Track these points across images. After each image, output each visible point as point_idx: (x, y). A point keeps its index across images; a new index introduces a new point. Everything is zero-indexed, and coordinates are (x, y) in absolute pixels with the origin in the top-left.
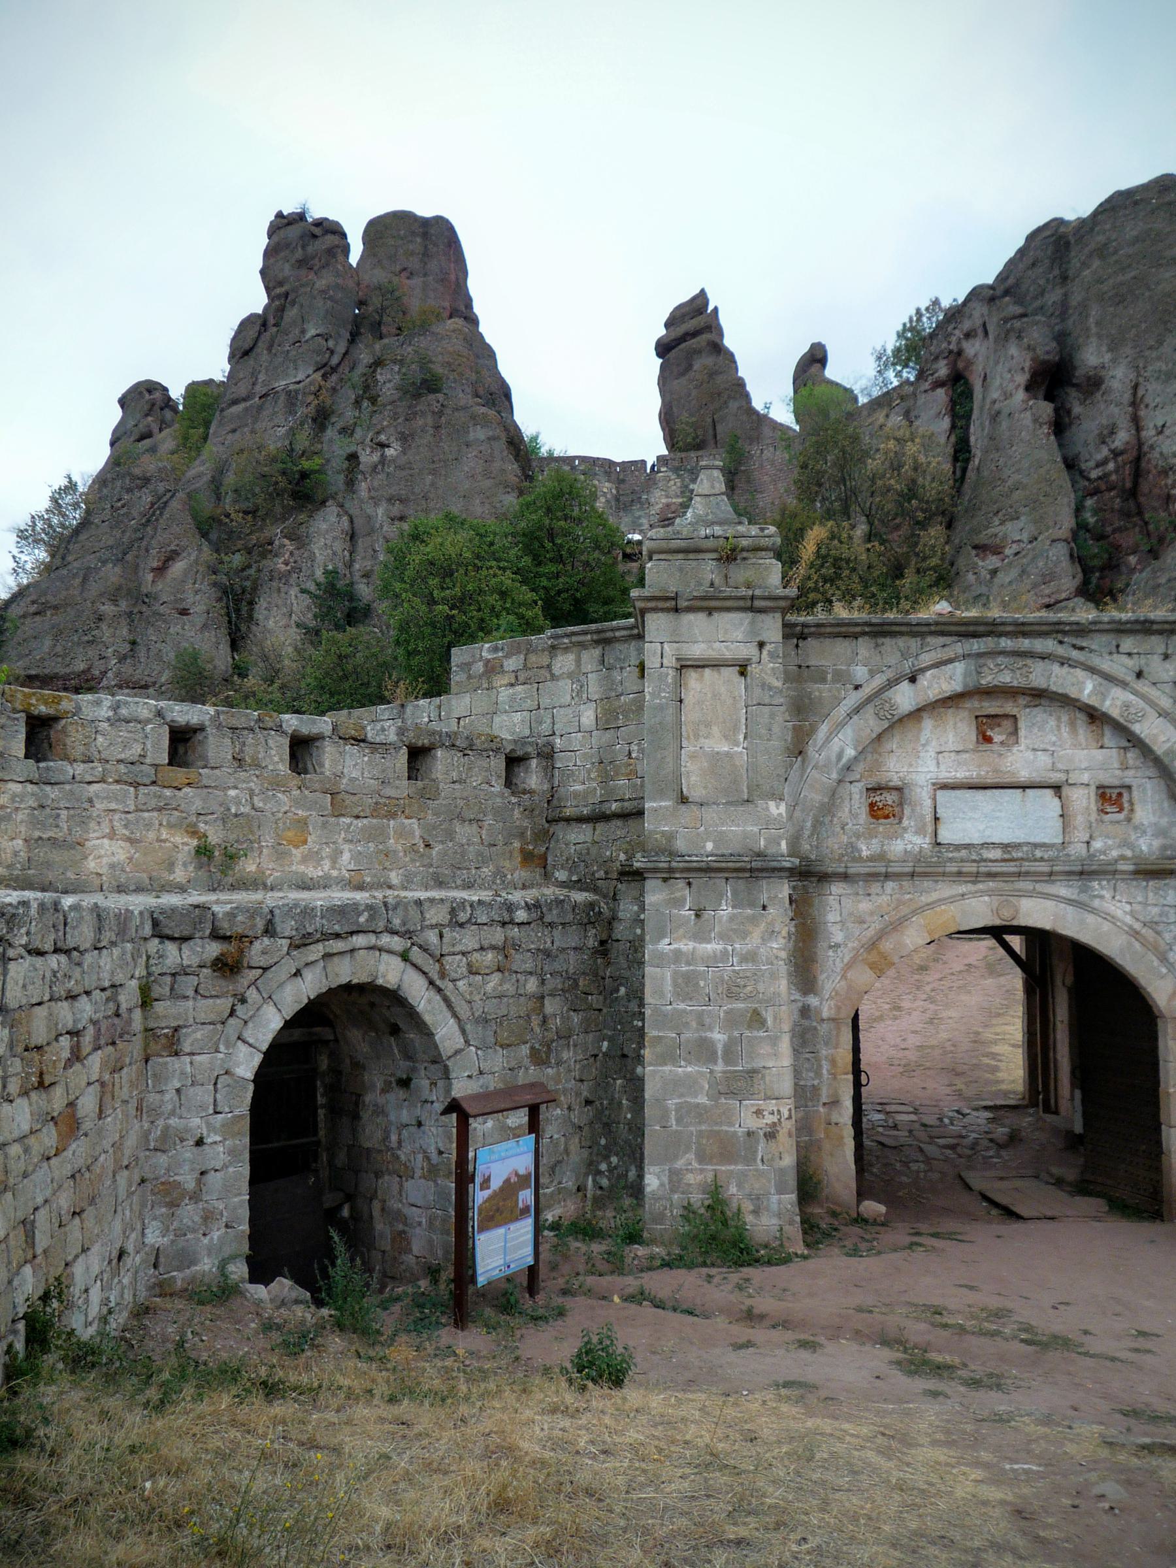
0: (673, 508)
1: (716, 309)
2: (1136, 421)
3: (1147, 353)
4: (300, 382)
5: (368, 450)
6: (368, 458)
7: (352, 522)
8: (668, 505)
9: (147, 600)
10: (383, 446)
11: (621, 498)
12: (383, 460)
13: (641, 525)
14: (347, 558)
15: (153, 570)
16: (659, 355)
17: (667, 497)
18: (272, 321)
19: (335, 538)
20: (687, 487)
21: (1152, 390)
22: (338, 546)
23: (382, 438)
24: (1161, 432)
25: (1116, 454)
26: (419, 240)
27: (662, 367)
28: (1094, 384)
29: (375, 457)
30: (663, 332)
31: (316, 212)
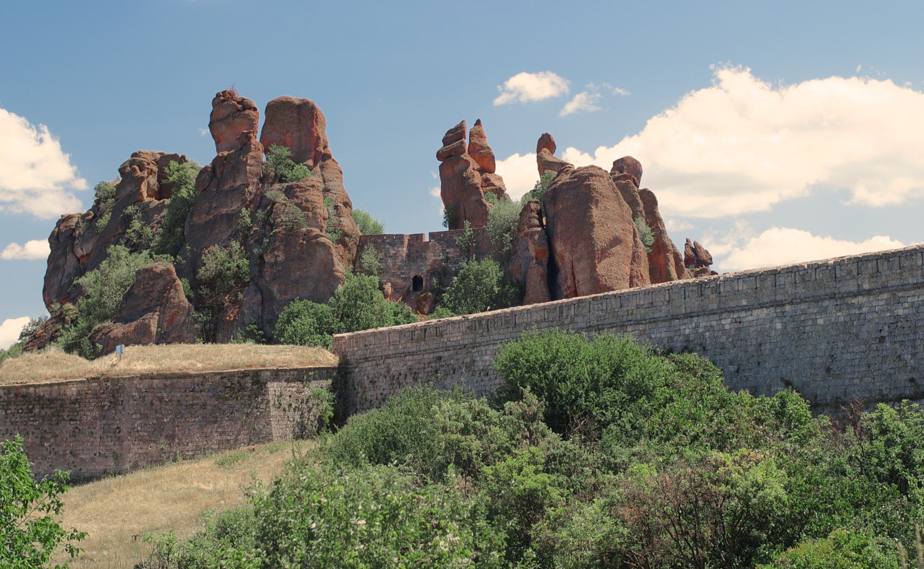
0: (437, 262)
1: (478, 123)
2: (573, 274)
3: (574, 249)
4: (233, 210)
5: (269, 257)
6: (268, 258)
7: (262, 293)
8: (435, 261)
9: (164, 336)
10: (276, 256)
11: (412, 255)
12: (276, 263)
13: (422, 270)
14: (260, 313)
15: (167, 321)
16: (439, 159)
17: (434, 256)
18: (218, 171)
19: (254, 303)
20: (444, 250)
21: (575, 264)
22: (255, 308)
23: (276, 253)
24: (578, 283)
25: (569, 287)
26: (295, 115)
27: (441, 167)
28: (562, 258)
29: (273, 260)
30: (441, 145)
31: (240, 94)
